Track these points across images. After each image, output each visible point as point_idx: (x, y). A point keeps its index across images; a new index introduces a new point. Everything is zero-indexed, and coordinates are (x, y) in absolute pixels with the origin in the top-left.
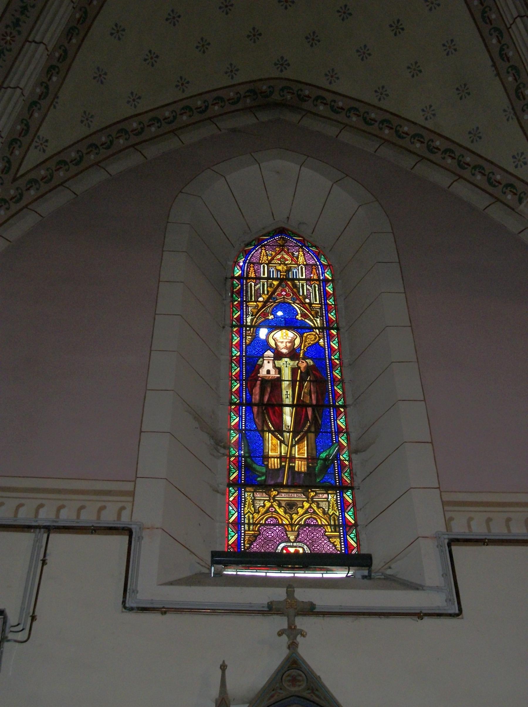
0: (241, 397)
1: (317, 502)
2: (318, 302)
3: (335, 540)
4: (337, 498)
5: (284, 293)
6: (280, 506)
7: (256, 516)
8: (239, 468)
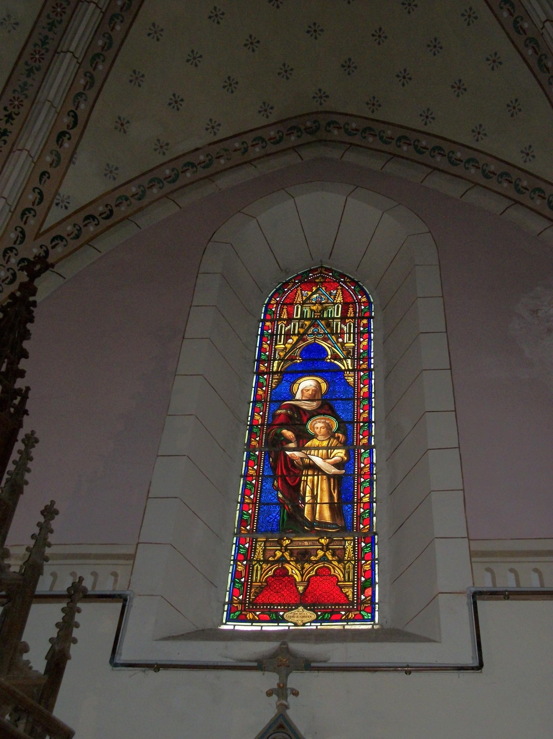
2: (352, 341)
3: (347, 590)
7: (264, 566)
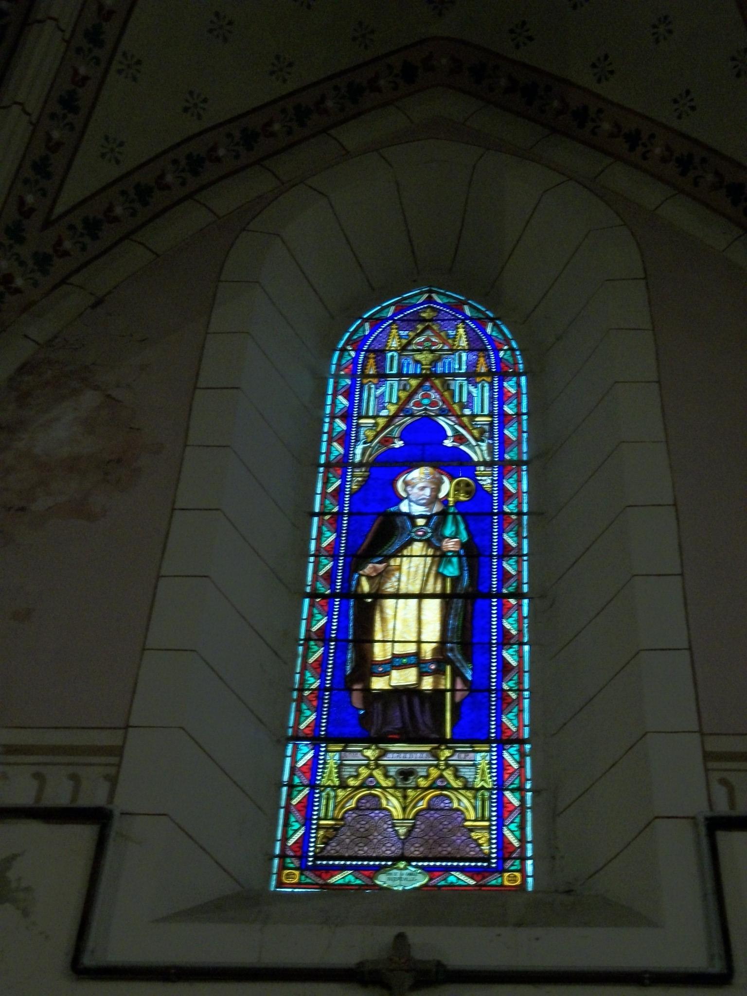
5: (426, 401)
6: (386, 776)
7: (341, 793)
8: (318, 710)
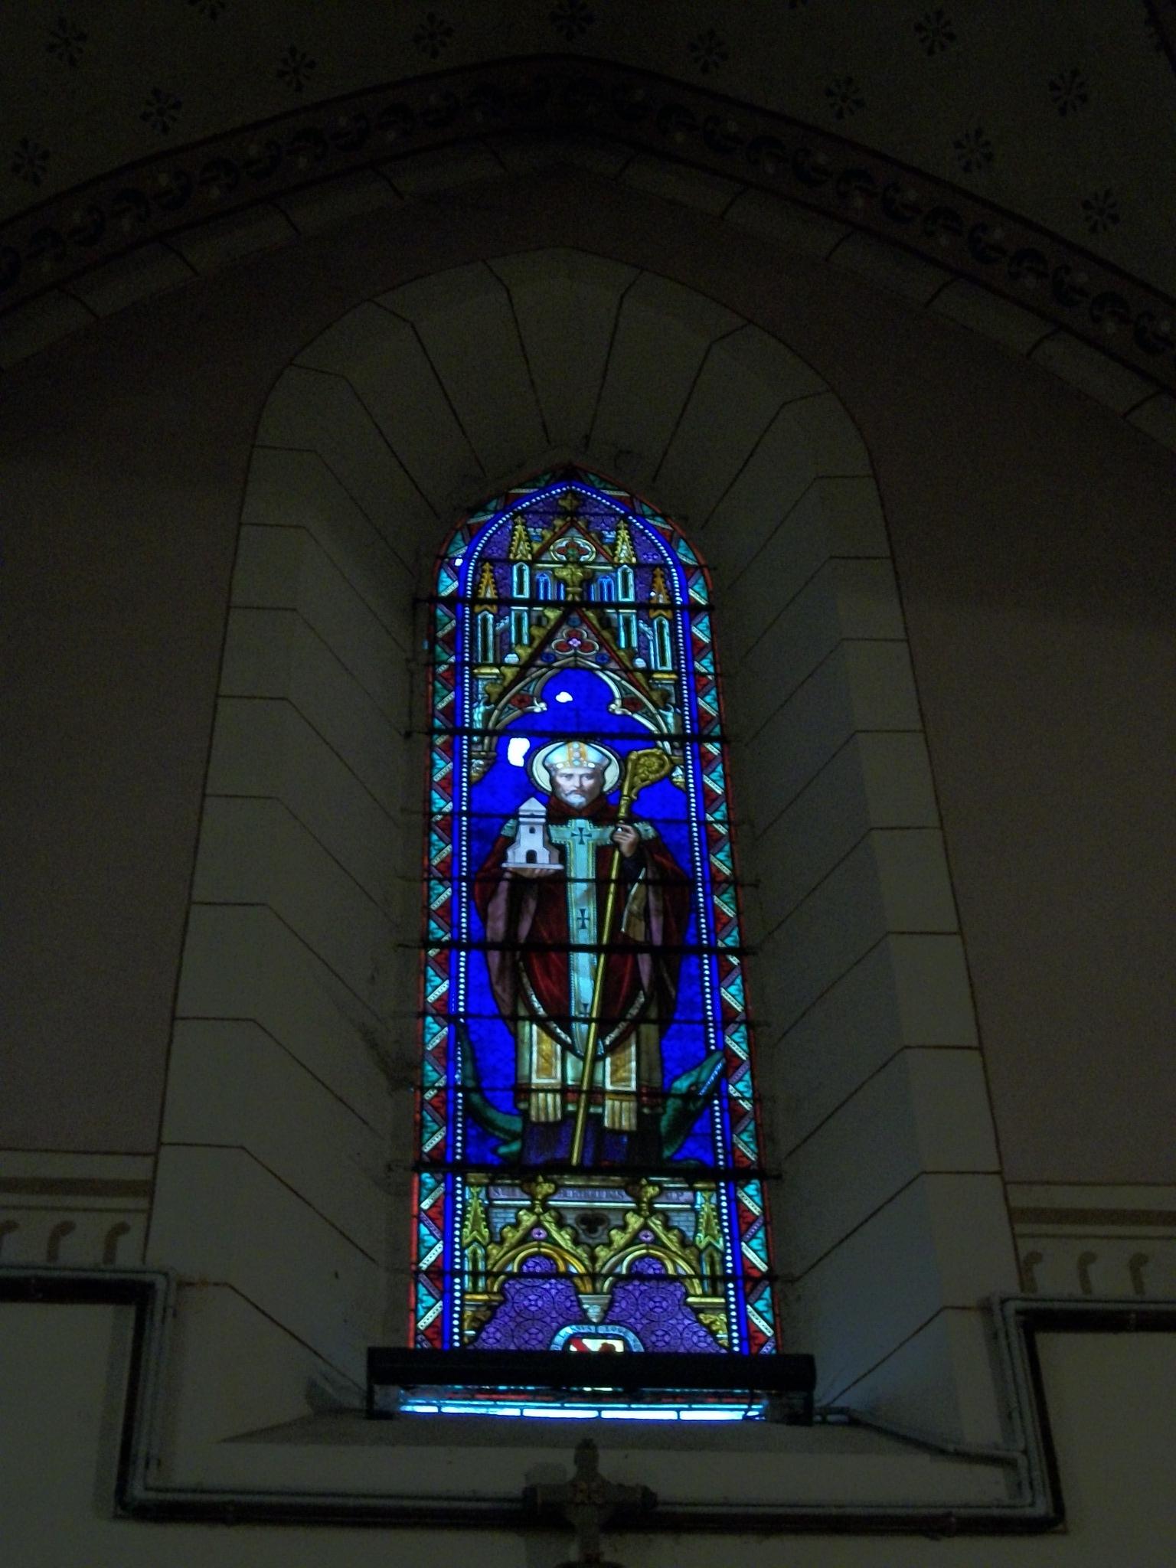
0: (454, 926)
1: (663, 1212)
2: (669, 667)
3: (713, 1317)
4: (719, 1201)
6: (561, 1224)
7: (494, 1251)
8: (449, 1121)
